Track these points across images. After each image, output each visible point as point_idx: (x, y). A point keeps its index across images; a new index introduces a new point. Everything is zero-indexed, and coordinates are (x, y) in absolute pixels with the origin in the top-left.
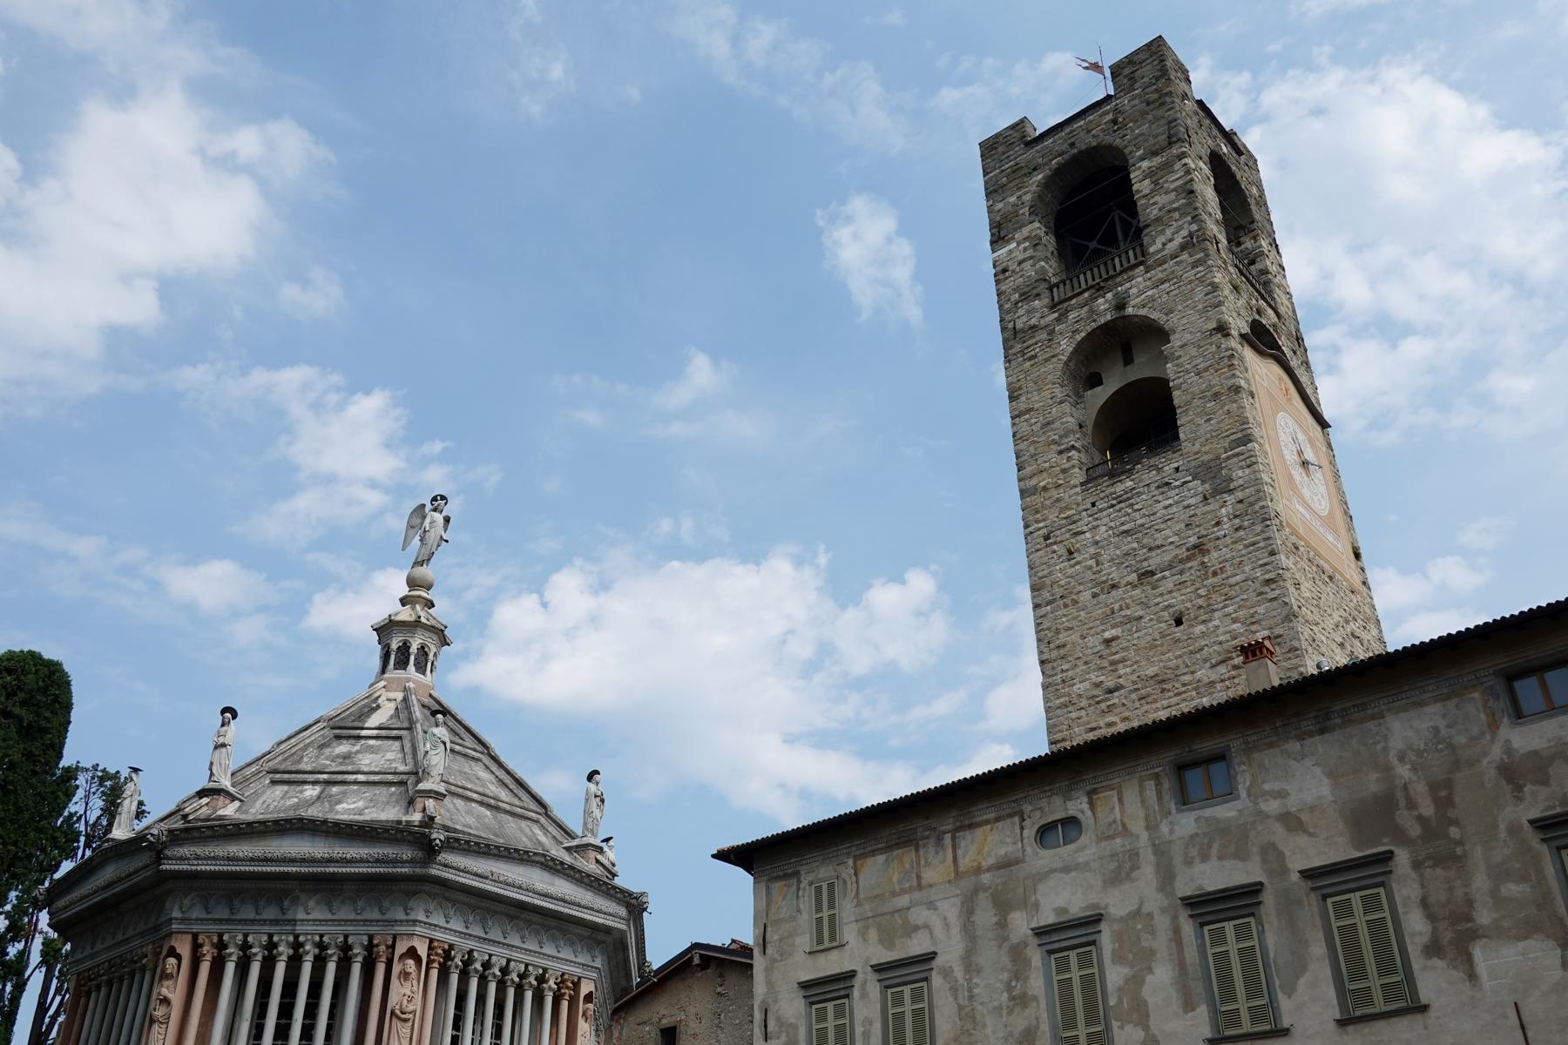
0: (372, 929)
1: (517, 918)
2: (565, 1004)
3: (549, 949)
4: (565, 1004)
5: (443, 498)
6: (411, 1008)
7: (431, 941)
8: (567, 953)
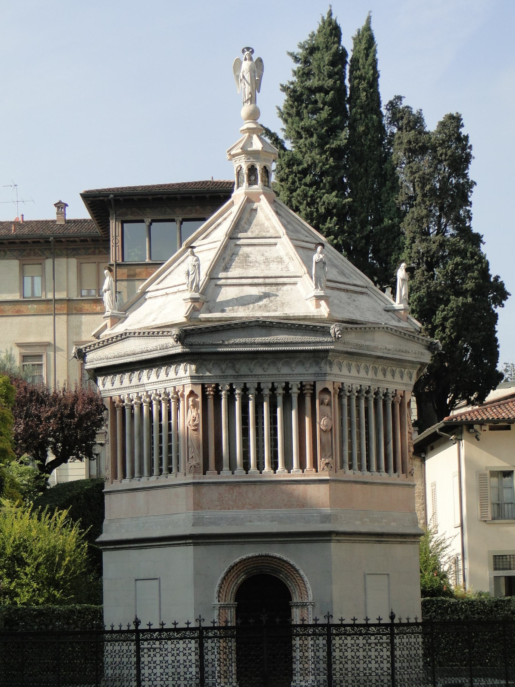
0: (174, 384)
1: (257, 359)
2: (308, 400)
3: (285, 370)
4: (308, 400)
5: (248, 49)
6: (196, 422)
7: (203, 385)
8: (299, 370)
